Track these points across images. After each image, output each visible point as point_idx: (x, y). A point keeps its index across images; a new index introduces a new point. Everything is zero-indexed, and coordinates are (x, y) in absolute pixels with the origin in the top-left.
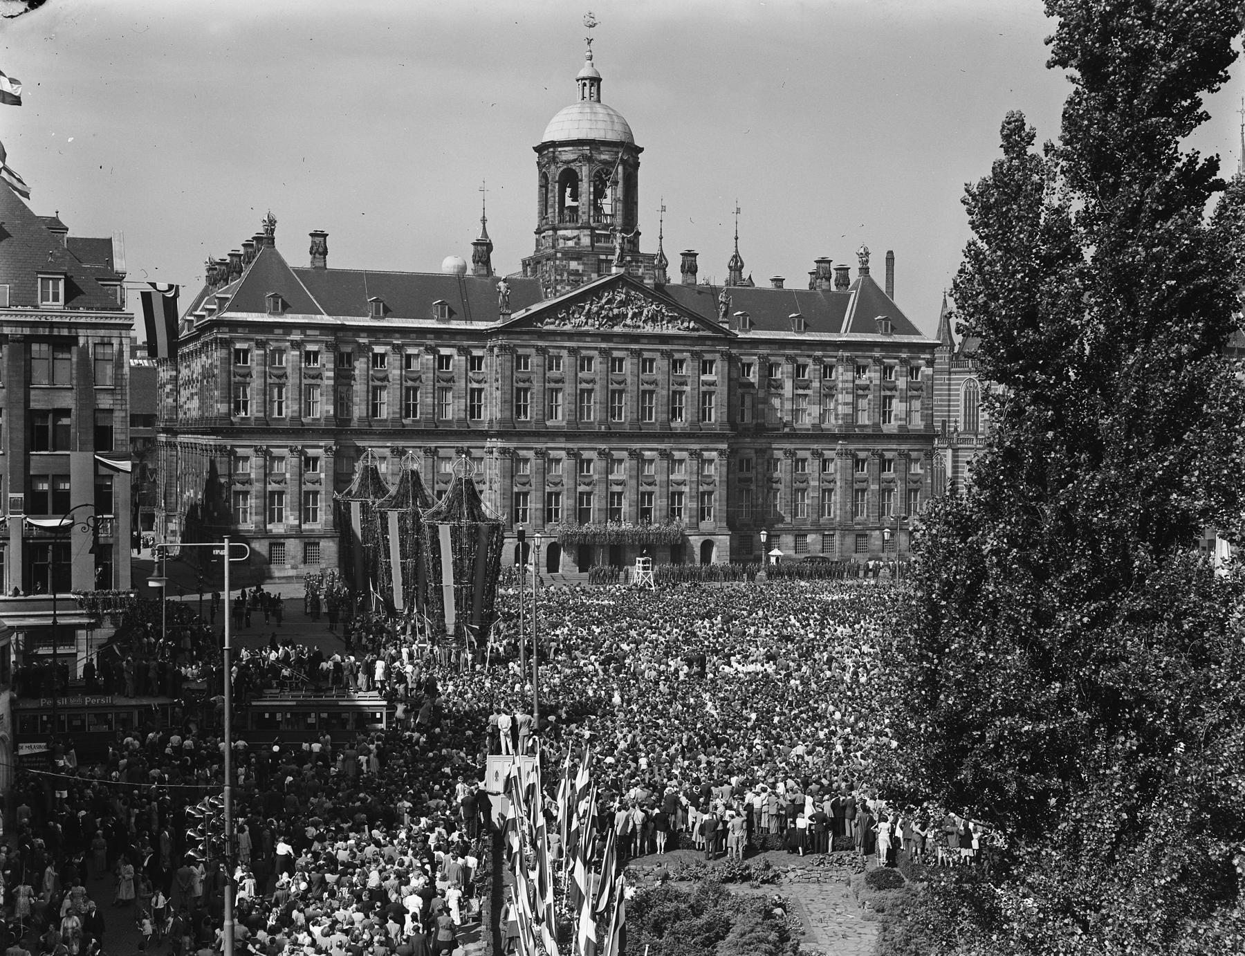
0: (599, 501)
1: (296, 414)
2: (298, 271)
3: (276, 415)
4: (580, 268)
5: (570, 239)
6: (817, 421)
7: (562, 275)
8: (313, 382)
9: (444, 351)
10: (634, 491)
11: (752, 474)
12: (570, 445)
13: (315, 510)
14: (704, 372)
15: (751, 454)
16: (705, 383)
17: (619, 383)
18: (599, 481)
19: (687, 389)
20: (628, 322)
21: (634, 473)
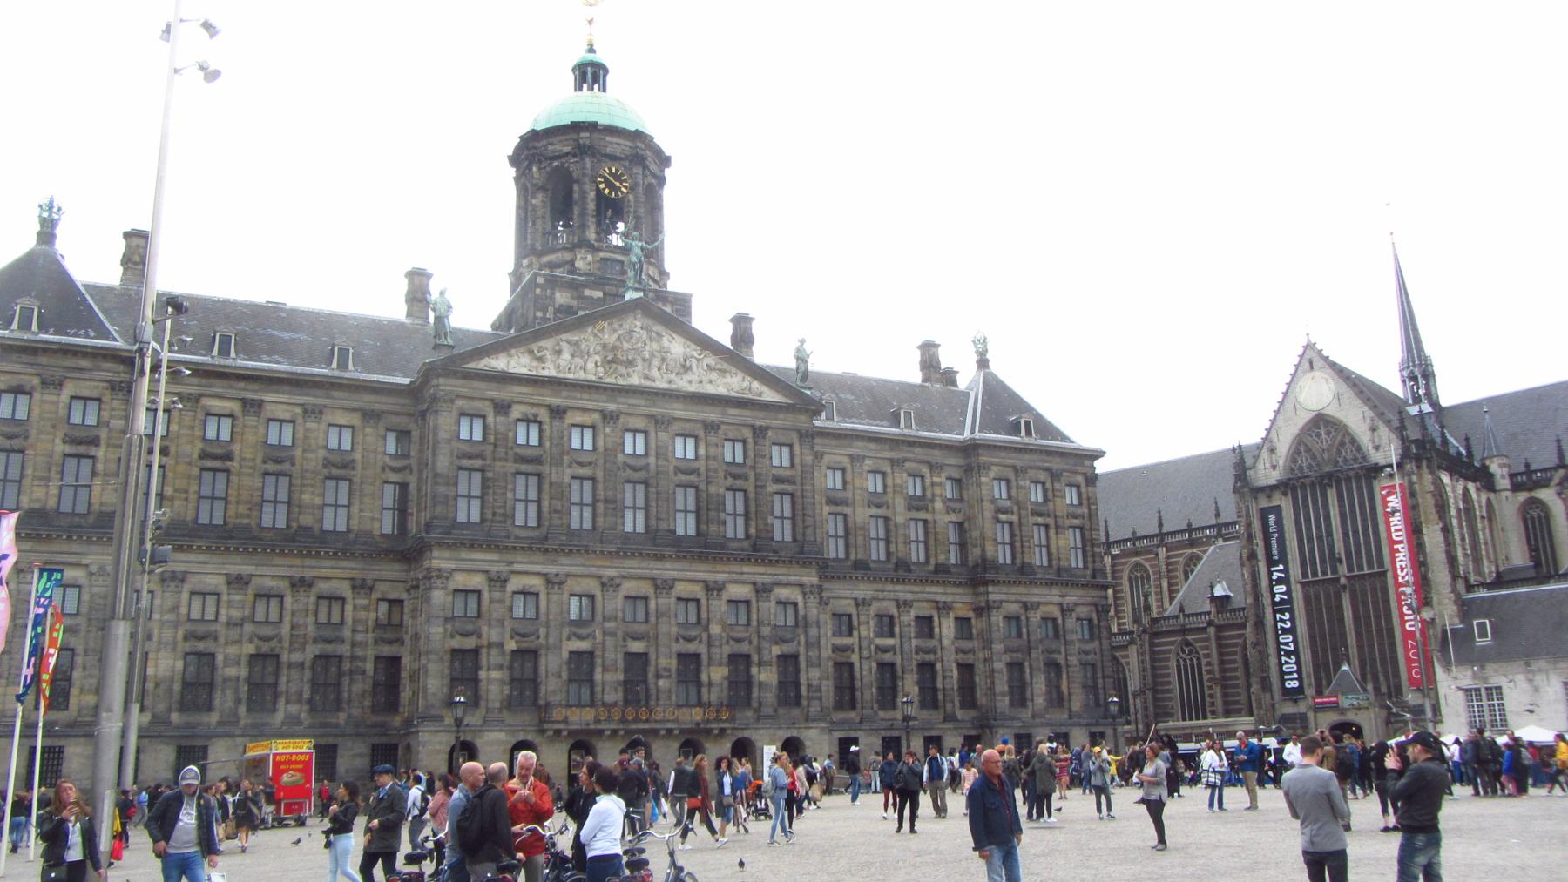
0: (605, 669)
1: (37, 506)
2: (85, 286)
4: (574, 303)
5: (559, 266)
7: (545, 310)
8: (82, 449)
12: (551, 569)
16: (778, 480)
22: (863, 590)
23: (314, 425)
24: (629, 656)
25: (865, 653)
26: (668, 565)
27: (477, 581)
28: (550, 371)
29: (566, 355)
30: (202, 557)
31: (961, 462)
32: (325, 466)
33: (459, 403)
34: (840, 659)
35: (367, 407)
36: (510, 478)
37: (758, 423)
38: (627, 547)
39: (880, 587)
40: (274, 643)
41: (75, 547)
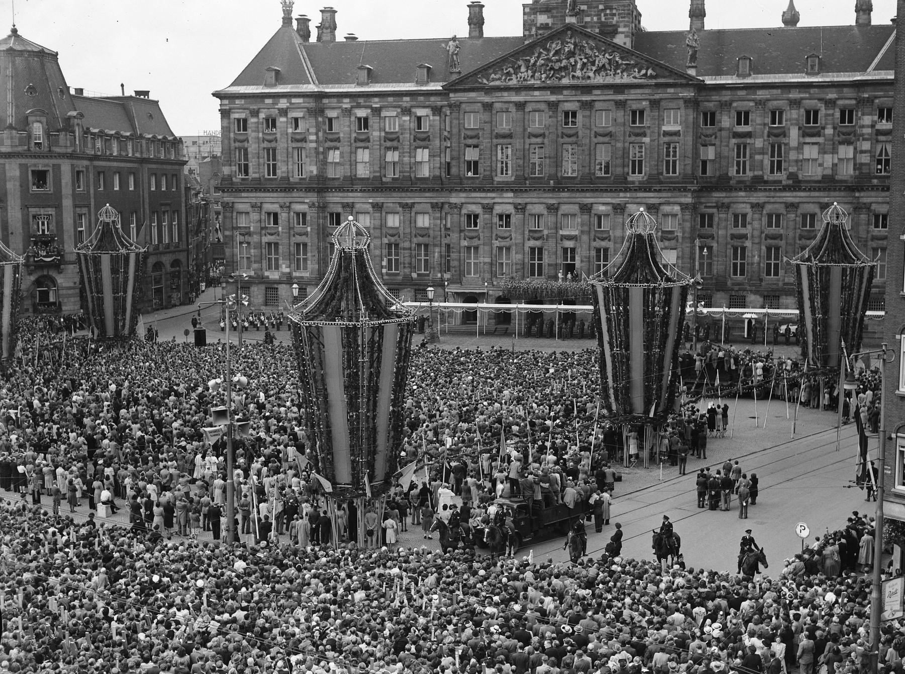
1: (284, 175)
3: (266, 176)
4: (550, 21)
6: (829, 172)
7: (530, 30)
8: (299, 145)
9: (420, 112)
10: (585, 246)
11: (748, 230)
13: (305, 260)
14: (669, 122)
15: (747, 209)
16: (666, 134)
17: (570, 136)
18: (547, 235)
19: (647, 140)
20: (578, 73)
21: (586, 228)
22: (759, 197)
23: (407, 118)
24: (565, 250)
25: (757, 241)
26: (588, 195)
27: (477, 209)
28: (514, 82)
29: (523, 69)
30: (359, 194)
31: (854, 95)
32: (415, 141)
33: (463, 106)
34: (735, 244)
35: (433, 104)
36: (494, 148)
37: (651, 97)
38: (561, 185)
39: (772, 194)
40: (396, 237)
41: (302, 194)
